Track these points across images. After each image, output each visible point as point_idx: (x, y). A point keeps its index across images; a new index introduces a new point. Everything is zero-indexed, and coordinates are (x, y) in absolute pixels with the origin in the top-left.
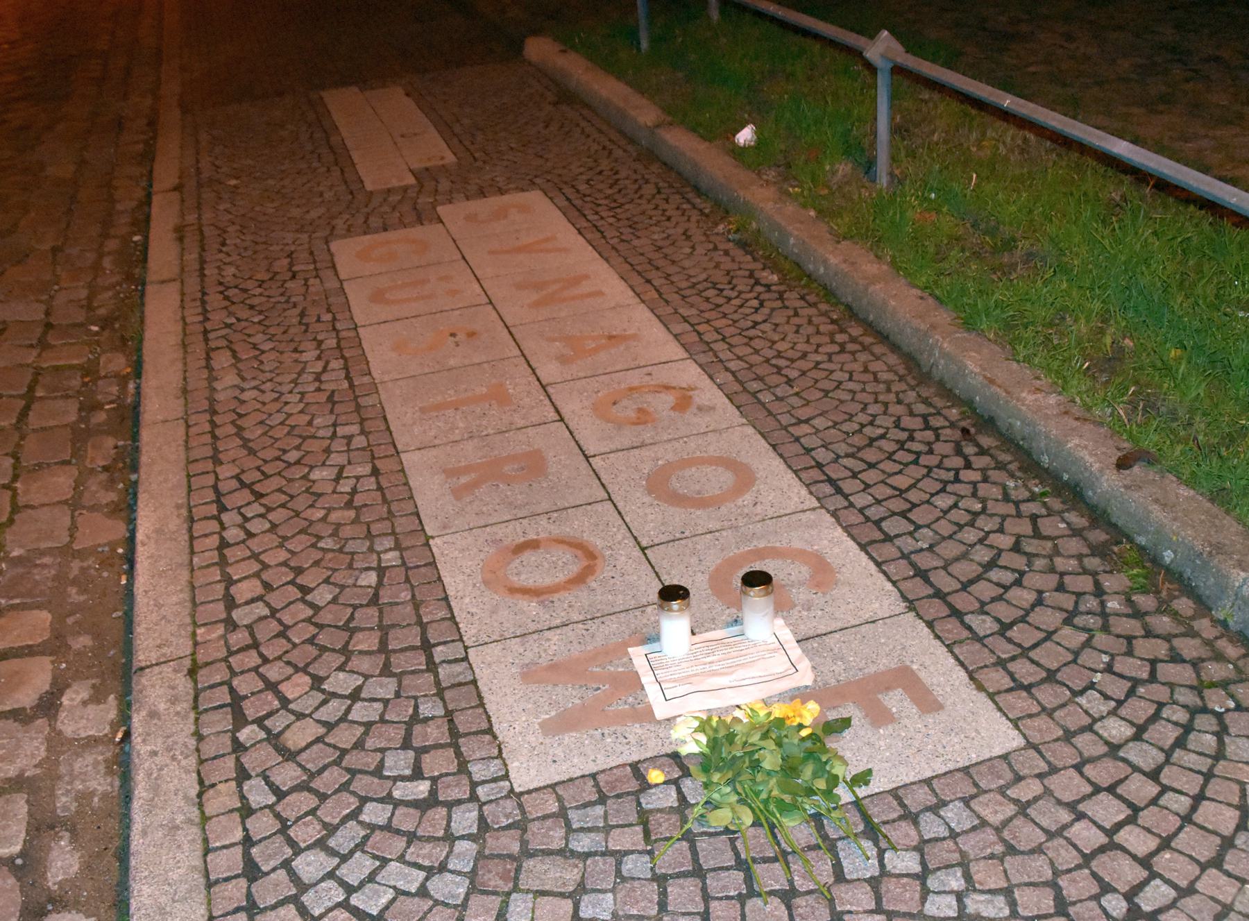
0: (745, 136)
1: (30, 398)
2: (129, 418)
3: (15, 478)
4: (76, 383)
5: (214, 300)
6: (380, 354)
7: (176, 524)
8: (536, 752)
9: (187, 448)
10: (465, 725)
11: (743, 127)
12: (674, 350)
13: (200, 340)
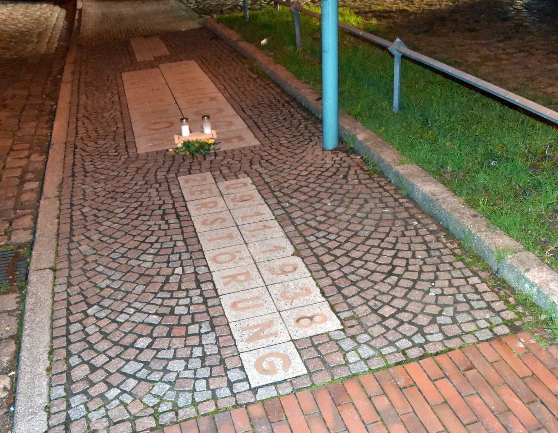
0: (264, 42)
1: (24, 109)
2: (53, 113)
3: (19, 123)
4: (38, 107)
5: (82, 85)
6: (129, 94)
7: (65, 124)
8: (144, 146)
9: (67, 137)
10: (129, 144)
11: (263, 39)
12: (216, 90)
13: (77, 92)
